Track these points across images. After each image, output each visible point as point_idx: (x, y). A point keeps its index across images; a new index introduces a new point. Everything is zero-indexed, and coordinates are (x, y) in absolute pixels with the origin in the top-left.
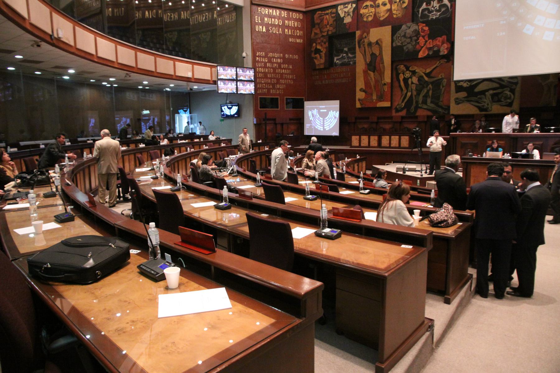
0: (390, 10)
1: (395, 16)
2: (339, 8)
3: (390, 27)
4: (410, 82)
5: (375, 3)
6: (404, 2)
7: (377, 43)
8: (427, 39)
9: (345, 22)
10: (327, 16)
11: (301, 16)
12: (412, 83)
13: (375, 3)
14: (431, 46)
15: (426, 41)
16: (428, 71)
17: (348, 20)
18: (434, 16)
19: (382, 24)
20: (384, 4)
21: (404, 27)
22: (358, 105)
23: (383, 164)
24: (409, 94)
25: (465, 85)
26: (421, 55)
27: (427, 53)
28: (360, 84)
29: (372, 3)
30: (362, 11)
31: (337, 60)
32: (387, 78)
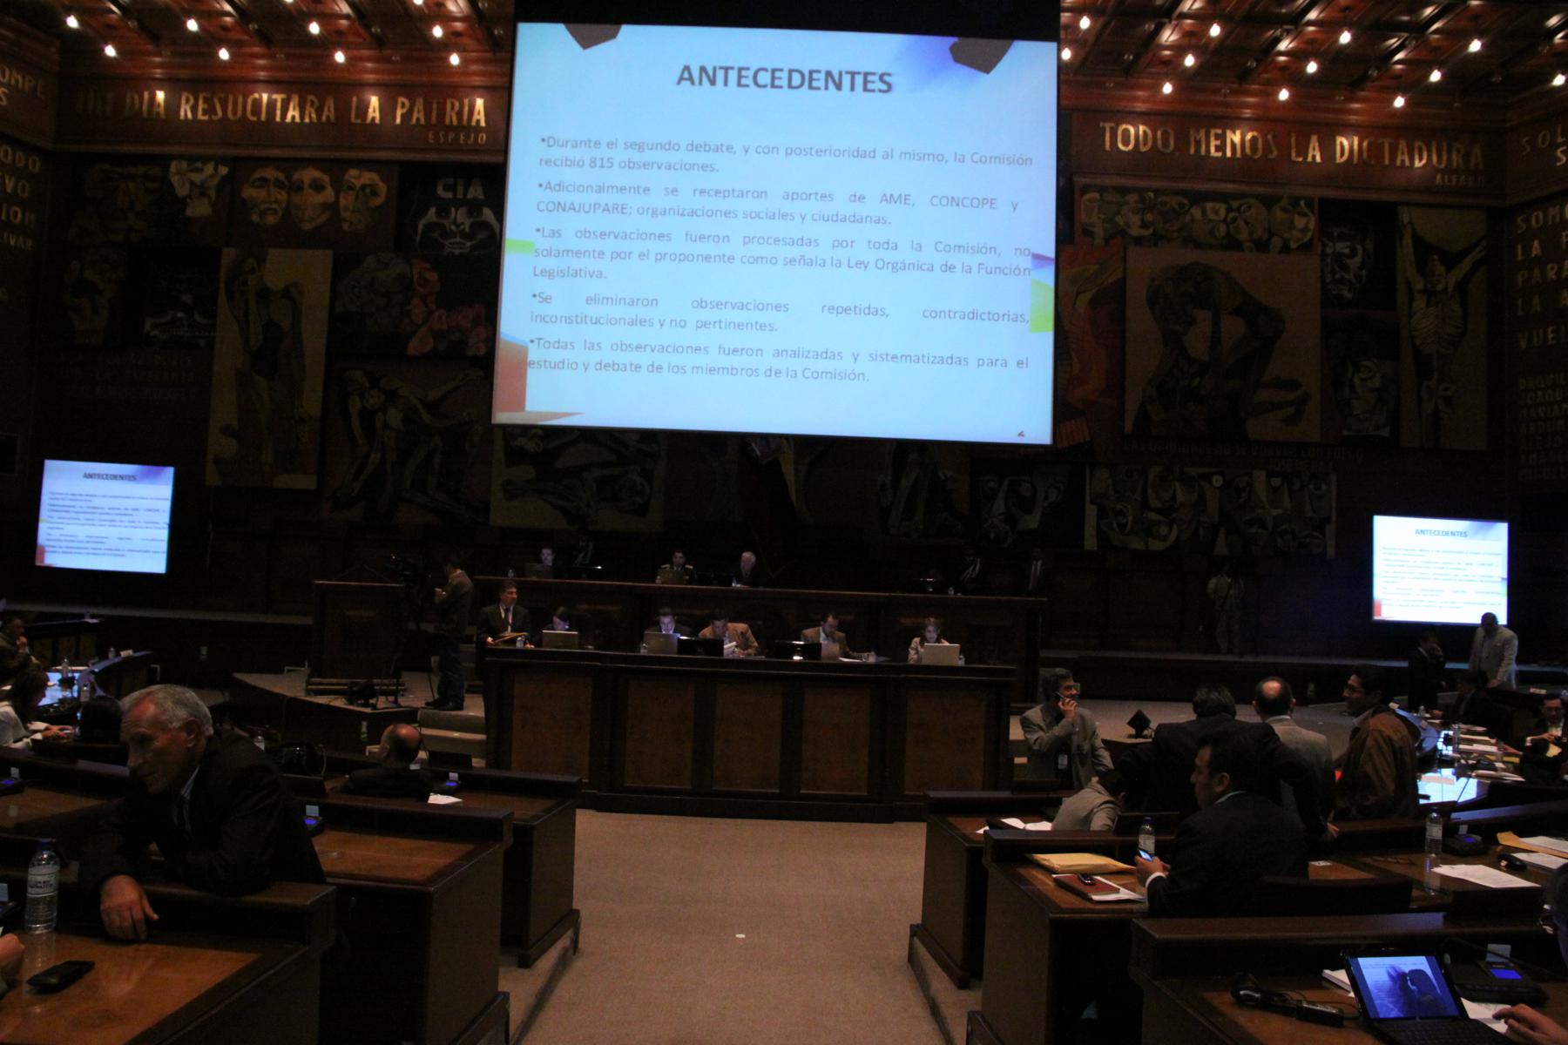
0: (333, 207)
1: (346, 226)
2: (173, 168)
3: (330, 252)
4: (379, 424)
5: (289, 178)
6: (375, 193)
7: (286, 293)
8: (433, 307)
9: (189, 212)
10: (131, 185)
11: (35, 165)
12: (386, 426)
13: (289, 178)
14: (445, 327)
15: (431, 313)
16: (433, 395)
17: (199, 209)
18: (456, 247)
19: (307, 241)
20: (318, 187)
21: (369, 261)
22: (213, 478)
23: (277, 670)
24: (375, 457)
25: (531, 446)
26: (414, 348)
27: (431, 343)
28: (224, 409)
29: (281, 176)
30: (249, 192)
31: (155, 326)
32: (312, 402)
